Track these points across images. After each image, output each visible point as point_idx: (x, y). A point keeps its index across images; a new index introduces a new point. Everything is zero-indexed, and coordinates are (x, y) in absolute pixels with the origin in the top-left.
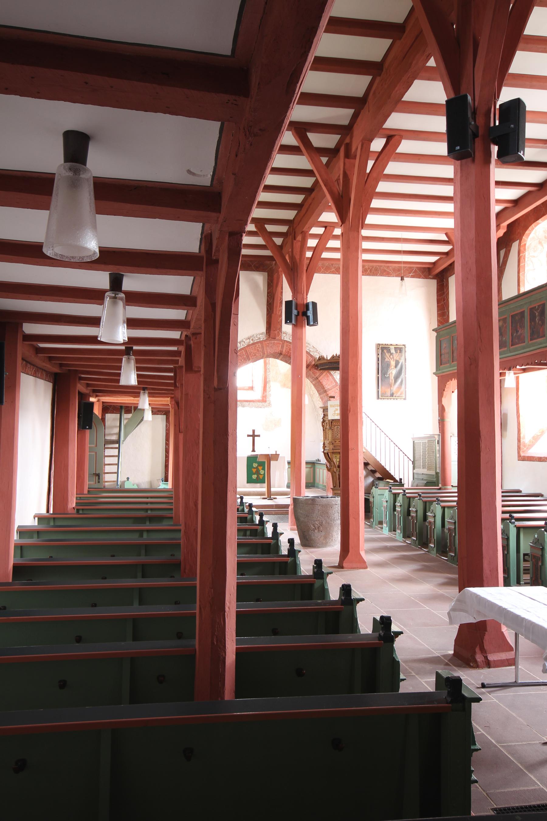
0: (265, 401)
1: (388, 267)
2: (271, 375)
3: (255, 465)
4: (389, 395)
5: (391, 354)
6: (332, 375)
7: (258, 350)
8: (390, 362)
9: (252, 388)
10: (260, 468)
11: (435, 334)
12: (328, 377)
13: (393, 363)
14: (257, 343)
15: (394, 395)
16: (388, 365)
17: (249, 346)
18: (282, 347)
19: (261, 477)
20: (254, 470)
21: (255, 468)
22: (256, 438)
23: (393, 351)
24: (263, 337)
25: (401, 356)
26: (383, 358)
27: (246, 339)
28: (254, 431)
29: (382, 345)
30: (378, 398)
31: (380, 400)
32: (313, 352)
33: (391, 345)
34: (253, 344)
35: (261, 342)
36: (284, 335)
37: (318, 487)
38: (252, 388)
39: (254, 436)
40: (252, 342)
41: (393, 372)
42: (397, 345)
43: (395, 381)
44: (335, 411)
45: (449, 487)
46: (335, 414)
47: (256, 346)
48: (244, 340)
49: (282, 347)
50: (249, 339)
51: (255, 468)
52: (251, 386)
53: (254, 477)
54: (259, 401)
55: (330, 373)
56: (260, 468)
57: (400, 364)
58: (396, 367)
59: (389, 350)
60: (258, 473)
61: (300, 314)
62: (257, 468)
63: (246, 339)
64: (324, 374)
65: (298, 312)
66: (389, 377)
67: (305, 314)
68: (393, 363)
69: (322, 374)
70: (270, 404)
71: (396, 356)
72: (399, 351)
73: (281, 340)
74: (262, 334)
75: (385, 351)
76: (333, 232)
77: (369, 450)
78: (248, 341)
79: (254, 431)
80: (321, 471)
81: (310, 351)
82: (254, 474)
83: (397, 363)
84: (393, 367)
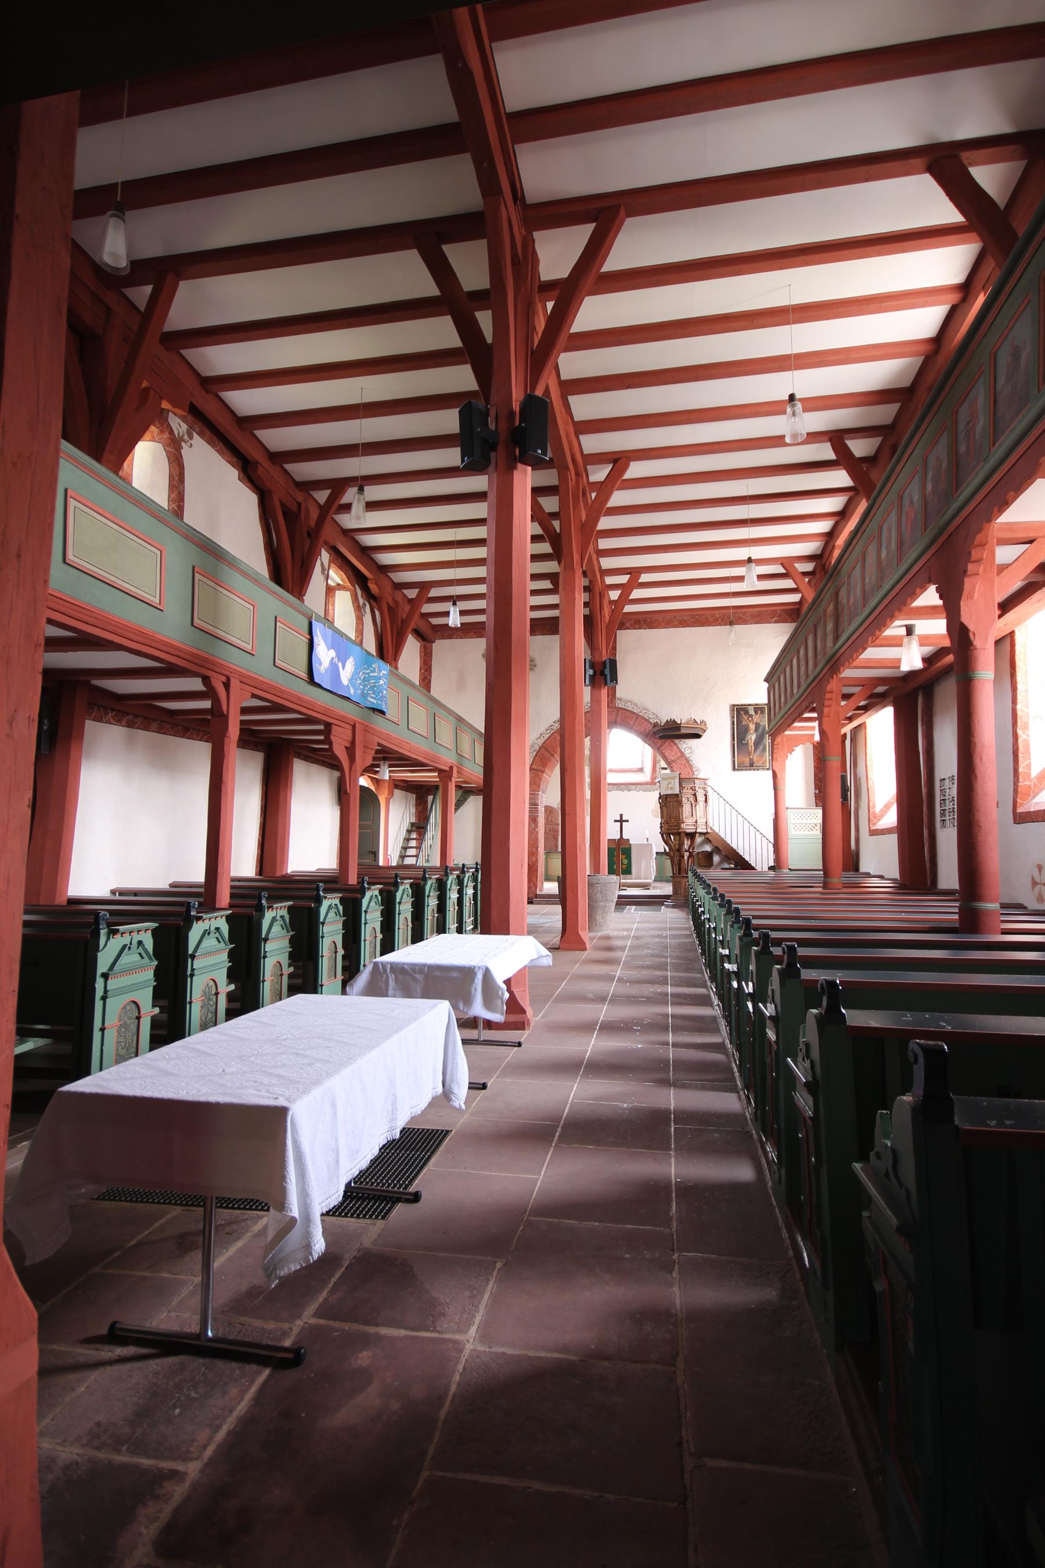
1: (745, 613)
5: (751, 716)
9: (641, 770)
11: (766, 685)
13: (752, 727)
16: (747, 730)
23: (752, 712)
28: (621, 816)
30: (734, 769)
38: (641, 770)
39: (621, 821)
41: (752, 737)
45: (786, 871)
54: (647, 784)
58: (756, 730)
59: (747, 712)
61: (598, 673)
65: (595, 672)
67: (602, 673)
68: (752, 727)
69: (664, 743)
71: (756, 718)
73: (615, 708)
76: (639, 578)
77: (717, 831)
79: (621, 816)
83: (757, 726)
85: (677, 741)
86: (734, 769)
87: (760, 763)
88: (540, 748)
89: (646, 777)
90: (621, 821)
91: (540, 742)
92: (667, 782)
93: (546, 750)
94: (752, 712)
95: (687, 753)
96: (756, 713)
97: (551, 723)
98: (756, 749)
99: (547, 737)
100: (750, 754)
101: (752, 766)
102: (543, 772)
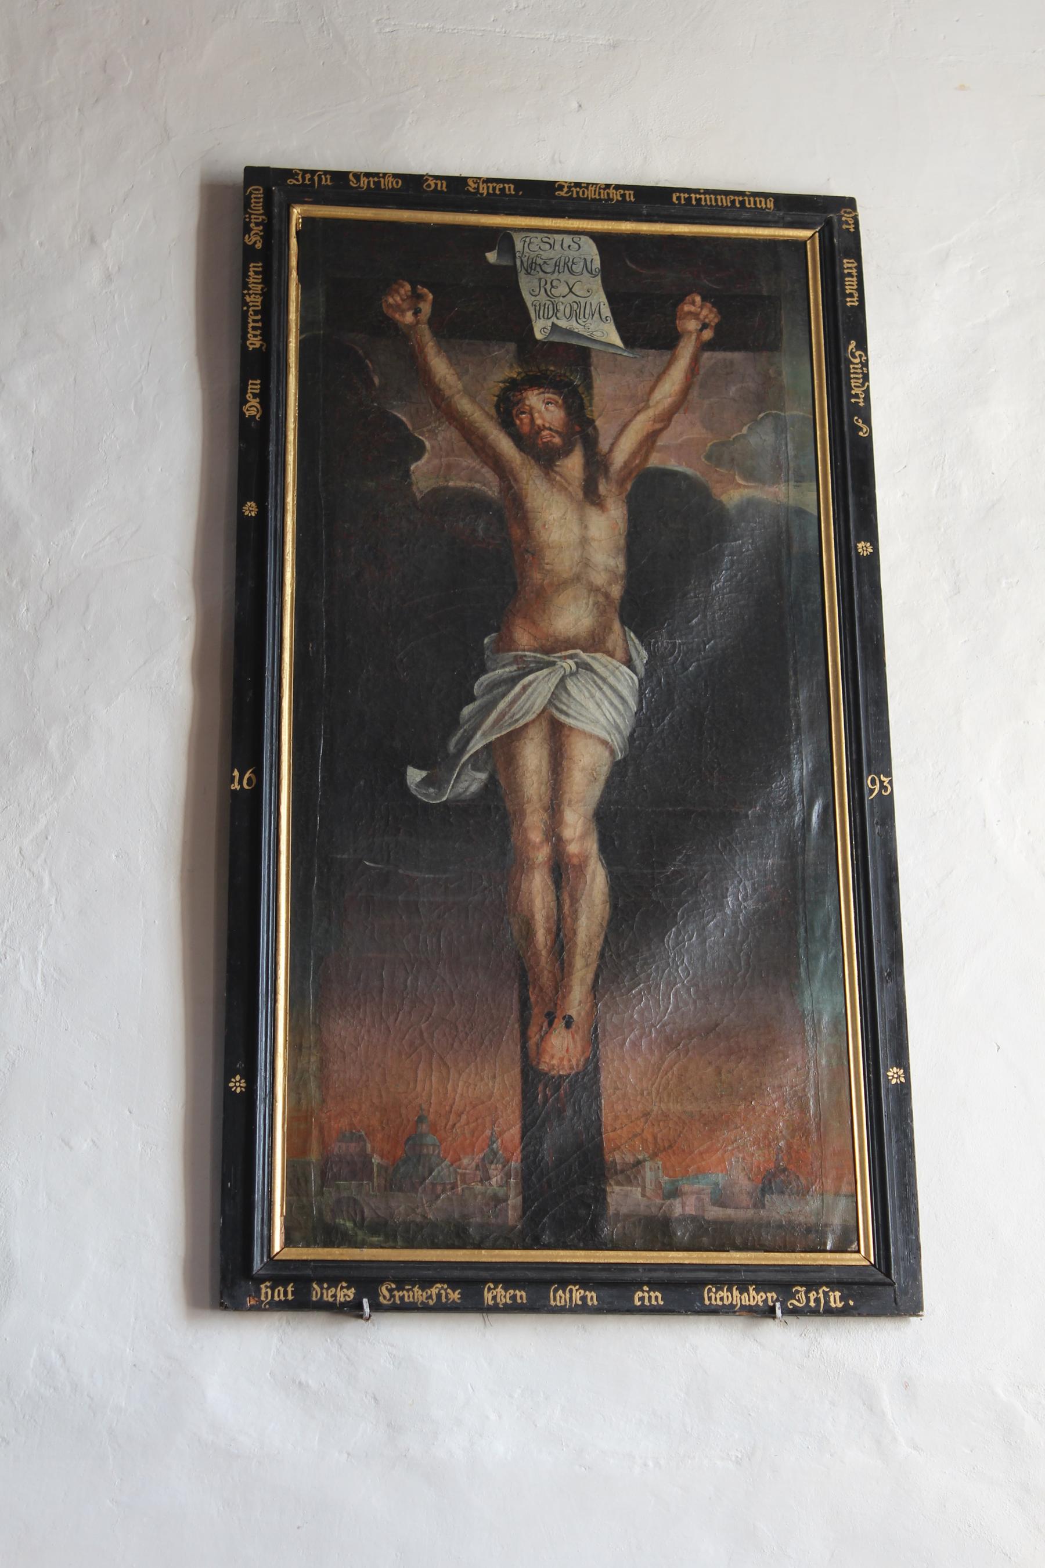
4: (501, 1187)
5: (565, 367)
8: (511, 512)
13: (579, 537)
15: (623, 1199)
16: (484, 578)
23: (574, 305)
25: (765, 399)
26: (358, 441)
29: (339, 186)
30: (233, 1272)
31: (261, 1348)
33: (538, 196)
42: (653, 200)
43: (642, 911)
57: (743, 546)
58: (644, 601)
66: (491, 814)
68: (579, 537)
71: (653, 408)
72: (696, 318)
75: (409, 308)
83: (669, 528)
84: (572, 616)
86: (233, 1272)
87: (725, 1172)
94: (574, 305)
96: (646, 323)
98: (642, 911)
100: (528, 993)
101: (564, 1229)
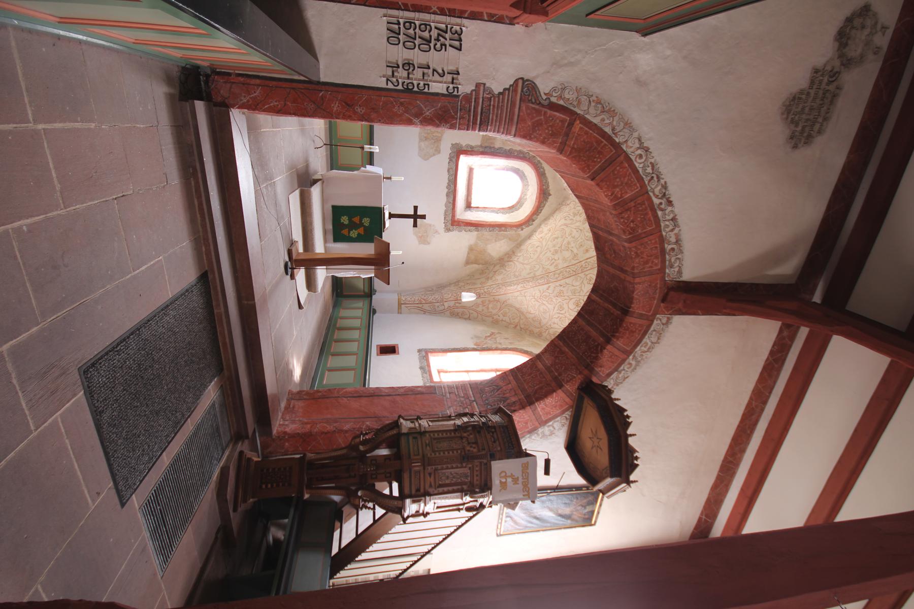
0: (452, 225)
2: (486, 233)
3: (366, 221)
6: (563, 412)
7: (646, 262)
9: (468, 206)
10: (361, 230)
12: (561, 406)
14: (663, 261)
17: (662, 240)
18: (641, 316)
19: (345, 232)
20: (356, 220)
21: (361, 220)
22: (412, 220)
23: (589, 509)
24: (671, 274)
27: (677, 236)
28: (423, 217)
32: (617, 378)
34: (663, 251)
35: (662, 270)
36: (664, 321)
37: (336, 305)
38: (468, 206)
40: (668, 247)
44: (512, 476)
46: (506, 477)
47: (657, 258)
48: (676, 231)
49: (641, 316)
50: (678, 241)
51: (361, 220)
52: (472, 205)
53: (345, 220)
55: (567, 410)
56: (361, 230)
60: (352, 226)
62: (361, 224)
63: (677, 236)
64: (568, 400)
70: (448, 230)
73: (654, 315)
74: (680, 272)
78: (673, 240)
79: (423, 217)
80: (358, 313)
81: (620, 373)
82: (350, 220)
85: (568, 414)
88: (617, 146)
89: (462, 214)
90: (416, 217)
91: (631, 148)
92: (518, 473)
93: (611, 162)
95: (546, 429)
97: (667, 177)
99: (638, 165)
102: (561, 151)
